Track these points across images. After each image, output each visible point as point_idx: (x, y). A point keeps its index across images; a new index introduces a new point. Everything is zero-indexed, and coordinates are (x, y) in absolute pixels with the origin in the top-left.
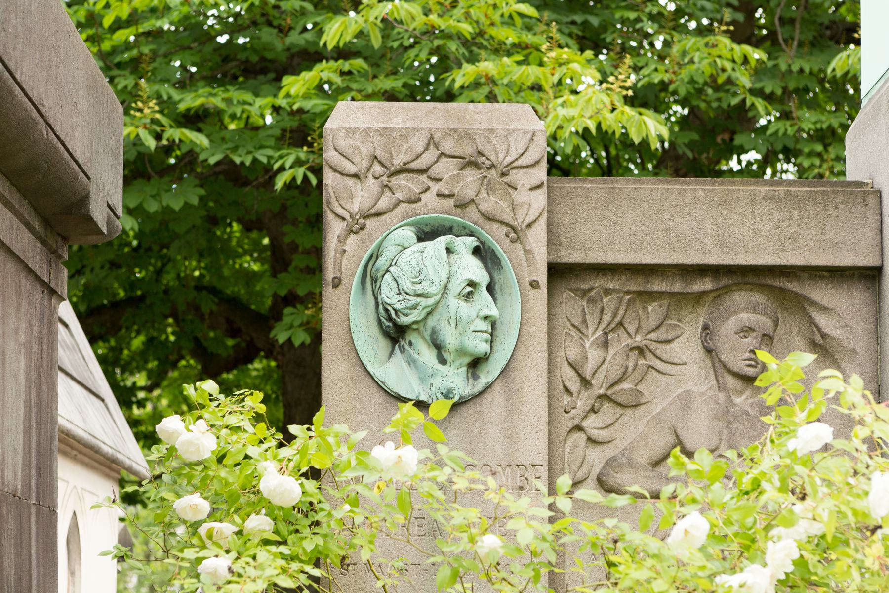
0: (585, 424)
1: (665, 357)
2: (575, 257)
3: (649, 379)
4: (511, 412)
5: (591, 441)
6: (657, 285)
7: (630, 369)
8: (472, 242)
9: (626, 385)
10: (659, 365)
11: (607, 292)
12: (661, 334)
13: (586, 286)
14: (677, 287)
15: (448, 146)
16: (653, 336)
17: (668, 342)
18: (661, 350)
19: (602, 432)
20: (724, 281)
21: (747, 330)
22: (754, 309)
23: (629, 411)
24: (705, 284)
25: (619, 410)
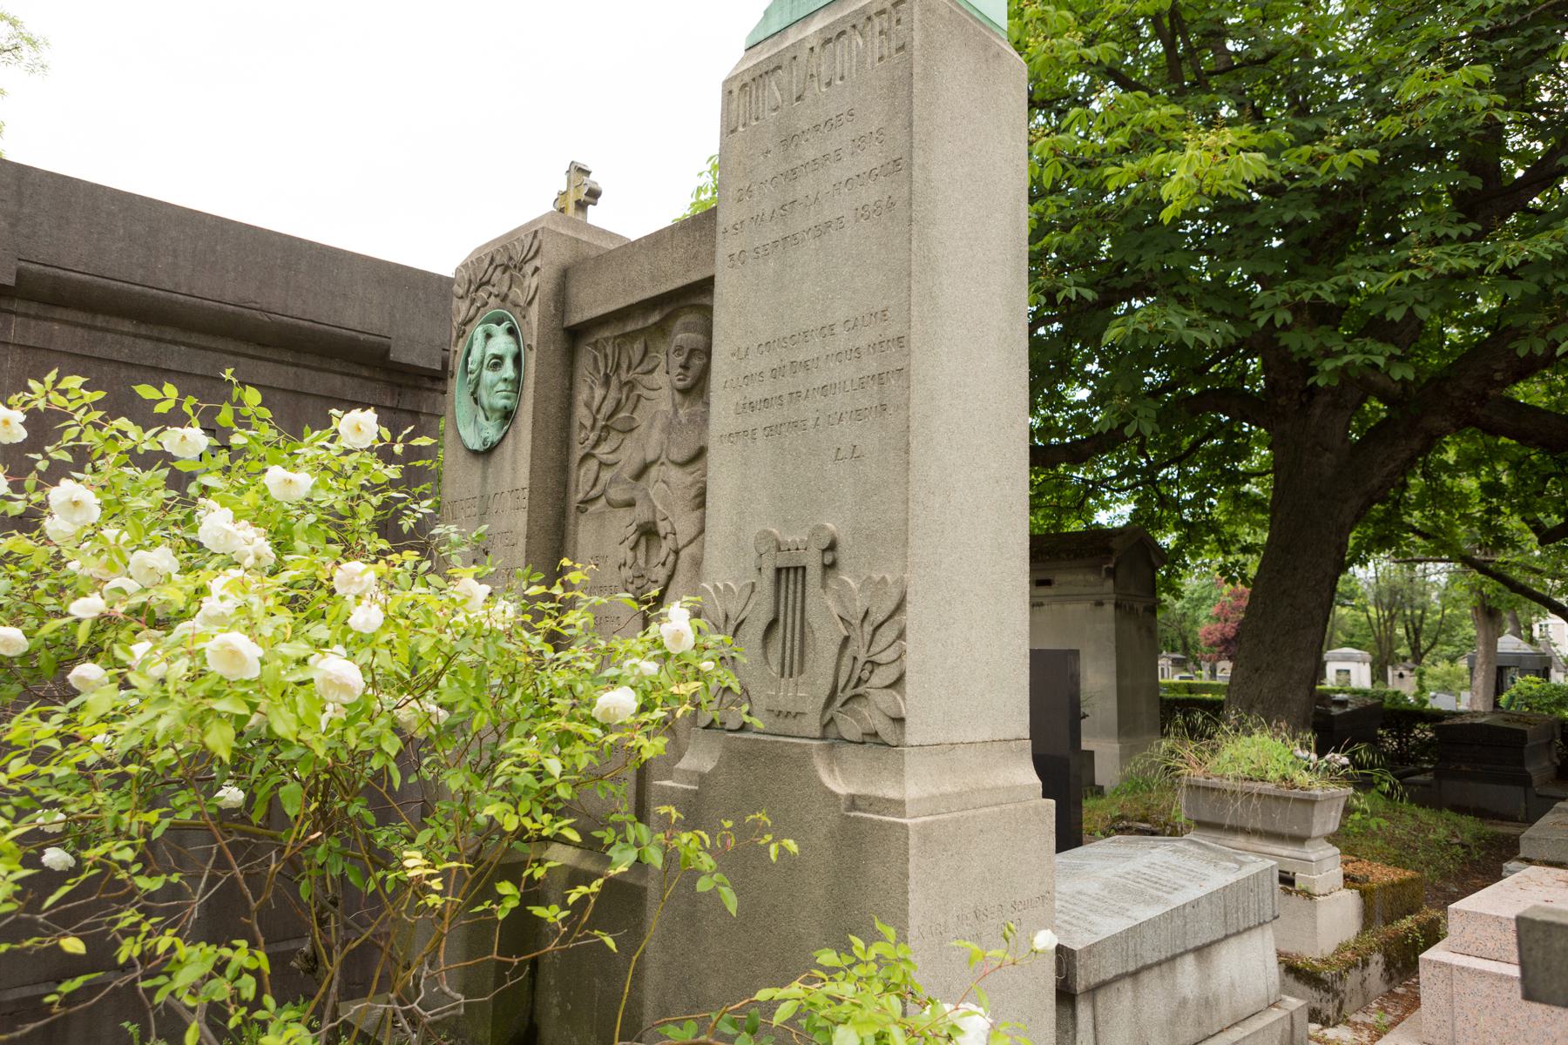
0: (596, 452)
1: (648, 385)
2: (576, 318)
3: (640, 406)
4: (515, 449)
5: (602, 464)
6: (630, 327)
7: (623, 401)
8: (506, 325)
9: (622, 415)
10: (645, 393)
11: (607, 340)
12: (645, 367)
13: (593, 340)
14: (640, 325)
15: (498, 261)
16: (639, 370)
17: (651, 372)
18: (646, 379)
19: (610, 456)
20: (667, 310)
21: (679, 349)
22: (686, 329)
23: (628, 435)
24: (655, 318)
25: (621, 436)
